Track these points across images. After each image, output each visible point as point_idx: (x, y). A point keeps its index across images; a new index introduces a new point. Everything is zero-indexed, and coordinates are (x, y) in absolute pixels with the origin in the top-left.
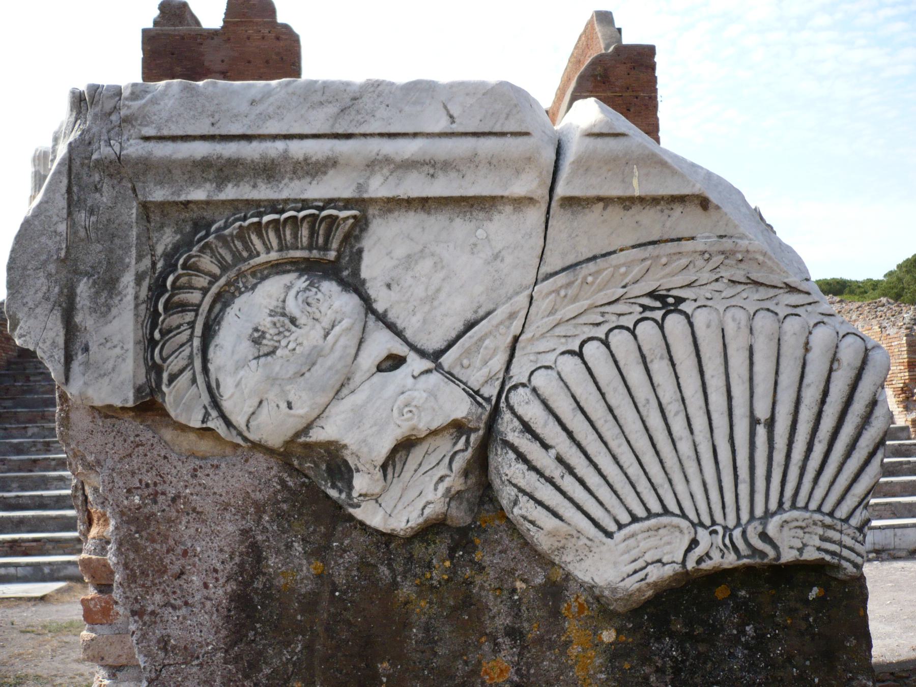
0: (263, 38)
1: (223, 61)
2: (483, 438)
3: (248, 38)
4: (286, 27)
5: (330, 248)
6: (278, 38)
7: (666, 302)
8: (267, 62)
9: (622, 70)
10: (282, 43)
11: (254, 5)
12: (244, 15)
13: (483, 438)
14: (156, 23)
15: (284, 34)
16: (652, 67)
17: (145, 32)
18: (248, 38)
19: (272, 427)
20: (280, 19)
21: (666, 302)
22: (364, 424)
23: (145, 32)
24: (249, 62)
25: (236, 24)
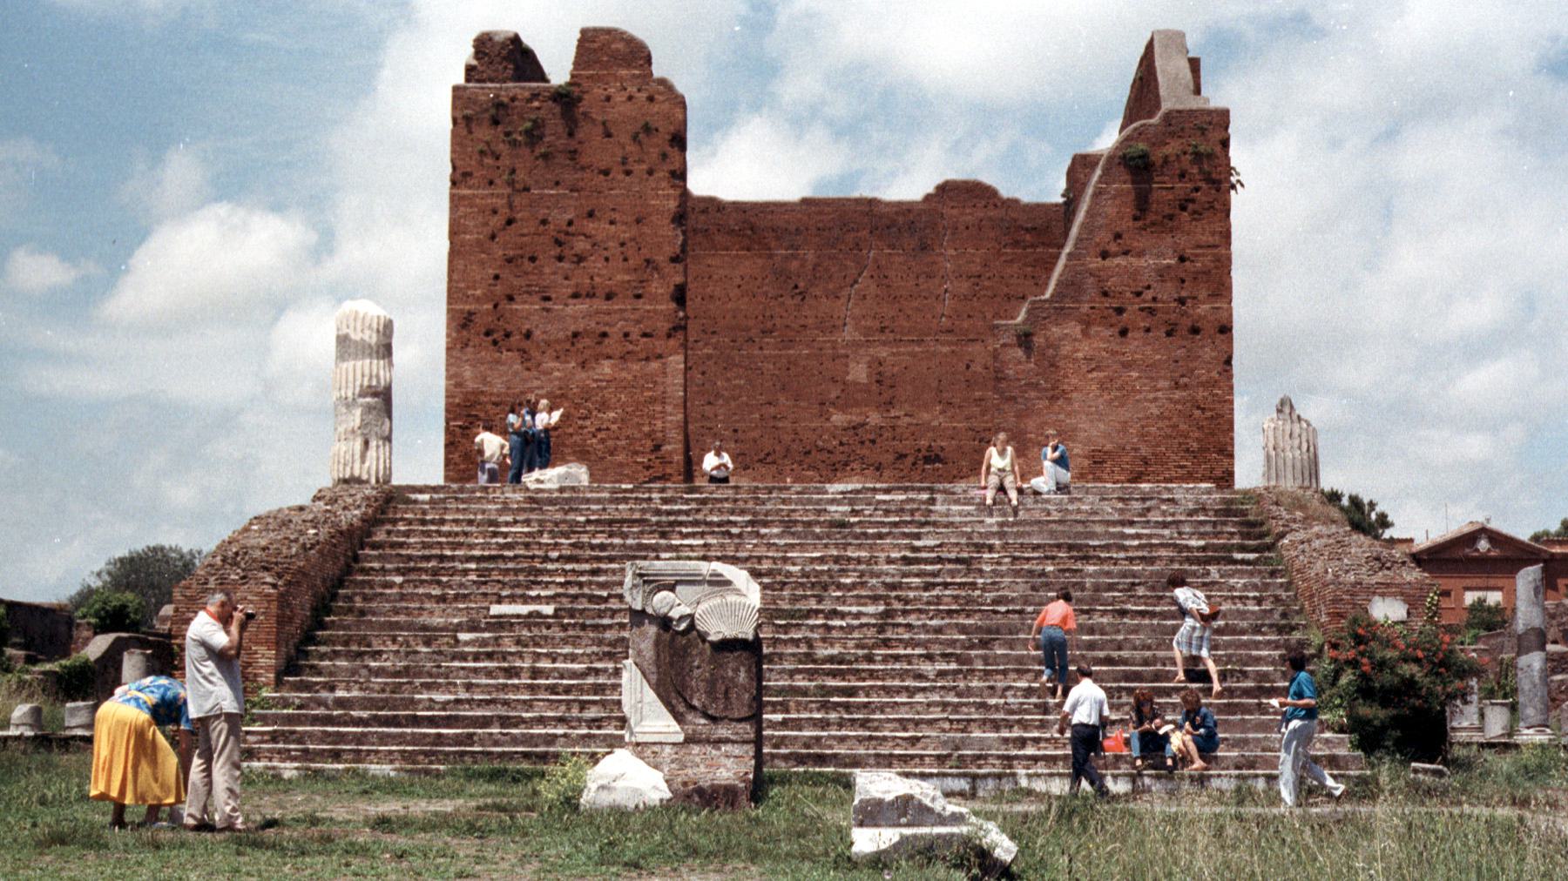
0: (630, 98)
2: (691, 616)
3: (608, 99)
4: (663, 82)
5: (672, 588)
10: (656, 108)
13: (691, 616)
14: (470, 70)
17: (456, 89)
18: (608, 99)
20: (658, 71)
22: (675, 614)
23: (456, 89)
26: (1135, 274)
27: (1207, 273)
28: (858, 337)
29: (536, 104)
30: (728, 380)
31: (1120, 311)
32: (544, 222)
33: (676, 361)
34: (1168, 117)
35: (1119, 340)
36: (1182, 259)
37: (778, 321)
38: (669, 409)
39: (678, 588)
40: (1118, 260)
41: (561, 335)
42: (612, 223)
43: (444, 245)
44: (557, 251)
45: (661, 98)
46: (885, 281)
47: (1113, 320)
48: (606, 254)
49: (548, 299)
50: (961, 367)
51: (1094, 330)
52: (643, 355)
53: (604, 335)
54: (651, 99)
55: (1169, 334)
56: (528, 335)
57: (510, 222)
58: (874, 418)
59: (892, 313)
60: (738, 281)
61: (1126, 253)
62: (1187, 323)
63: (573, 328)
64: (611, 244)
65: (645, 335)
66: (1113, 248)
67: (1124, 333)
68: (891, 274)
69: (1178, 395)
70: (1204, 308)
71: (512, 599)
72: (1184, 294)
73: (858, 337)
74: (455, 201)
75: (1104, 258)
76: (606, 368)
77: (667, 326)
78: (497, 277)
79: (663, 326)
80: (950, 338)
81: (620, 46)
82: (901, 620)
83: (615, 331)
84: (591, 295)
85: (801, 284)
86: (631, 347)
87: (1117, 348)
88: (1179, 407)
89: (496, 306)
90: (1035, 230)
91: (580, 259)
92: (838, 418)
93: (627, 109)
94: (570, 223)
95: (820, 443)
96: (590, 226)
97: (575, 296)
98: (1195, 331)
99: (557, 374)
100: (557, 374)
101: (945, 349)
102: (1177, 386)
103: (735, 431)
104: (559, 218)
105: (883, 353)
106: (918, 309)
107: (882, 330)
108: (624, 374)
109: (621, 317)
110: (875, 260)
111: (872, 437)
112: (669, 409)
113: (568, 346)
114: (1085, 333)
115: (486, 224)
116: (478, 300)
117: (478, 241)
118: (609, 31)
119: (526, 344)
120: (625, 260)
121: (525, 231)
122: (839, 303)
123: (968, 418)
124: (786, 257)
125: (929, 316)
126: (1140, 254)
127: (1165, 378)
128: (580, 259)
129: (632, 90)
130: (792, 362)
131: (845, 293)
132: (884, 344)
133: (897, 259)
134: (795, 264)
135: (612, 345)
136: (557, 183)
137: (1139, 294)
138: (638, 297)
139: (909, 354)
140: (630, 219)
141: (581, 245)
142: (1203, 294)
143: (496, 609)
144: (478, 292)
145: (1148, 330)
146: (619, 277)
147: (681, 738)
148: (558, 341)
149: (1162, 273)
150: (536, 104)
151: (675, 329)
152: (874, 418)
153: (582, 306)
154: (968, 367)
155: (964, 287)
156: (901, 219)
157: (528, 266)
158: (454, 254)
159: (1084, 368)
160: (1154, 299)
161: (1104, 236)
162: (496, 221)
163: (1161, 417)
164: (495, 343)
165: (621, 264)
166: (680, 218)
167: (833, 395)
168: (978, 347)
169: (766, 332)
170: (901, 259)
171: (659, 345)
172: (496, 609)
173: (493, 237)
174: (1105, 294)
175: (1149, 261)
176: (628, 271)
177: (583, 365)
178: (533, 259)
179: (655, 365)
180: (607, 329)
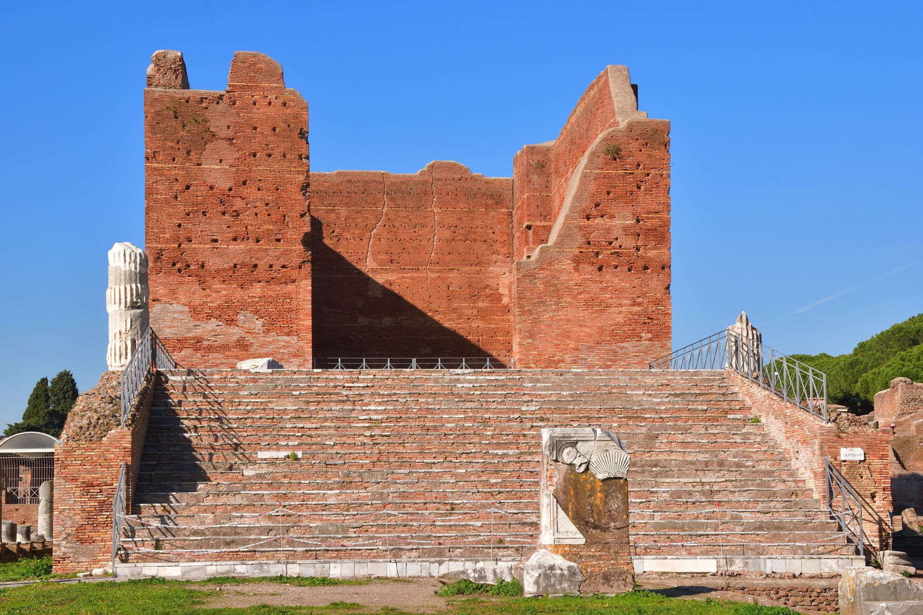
0: (270, 104)
1: (229, 127)
5: (574, 444)
6: (284, 104)
7: (607, 451)
8: (274, 129)
9: (634, 146)
11: (261, 69)
12: (251, 79)
13: (588, 463)
15: (293, 101)
16: (666, 145)
18: (255, 104)
19: (568, 462)
21: (607, 451)
22: (577, 462)
24: (255, 128)
25: (242, 87)
26: (608, 230)
27: (656, 229)
28: (375, 266)
29: (204, 105)
31: (597, 254)
32: (212, 188)
33: (306, 285)
34: (630, 127)
35: (598, 273)
36: (638, 221)
38: (301, 317)
39: (579, 445)
40: (598, 220)
41: (226, 266)
42: (259, 190)
43: (143, 204)
44: (222, 208)
45: (291, 104)
46: (394, 229)
47: (595, 261)
48: (255, 210)
49: (216, 241)
51: (582, 266)
52: (283, 280)
53: (256, 266)
54: (284, 104)
55: (630, 270)
56: (203, 266)
57: (188, 187)
61: (602, 216)
62: (640, 263)
63: (234, 261)
64: (259, 204)
65: (284, 267)
66: (594, 212)
67: (600, 269)
68: (397, 225)
69: (636, 309)
70: (651, 254)
71: (269, 447)
72: (640, 243)
73: (375, 266)
74: (150, 171)
75: (588, 219)
76: (257, 290)
77: (300, 260)
78: (180, 225)
79: (297, 261)
81: (262, 65)
82: (529, 458)
83: (263, 264)
84: (245, 238)
85: (337, 231)
86: (274, 275)
87: (597, 278)
88: (636, 317)
89: (179, 246)
90: (495, 197)
91: (237, 214)
92: (362, 320)
93: (270, 111)
94: (230, 190)
96: (245, 191)
97: (235, 239)
98: (646, 268)
99: (224, 293)
100: (224, 293)
102: (635, 304)
104: (223, 184)
106: (415, 248)
108: (270, 293)
109: (269, 254)
110: (387, 214)
112: (301, 317)
113: (230, 273)
114: (576, 269)
115: (171, 189)
116: (167, 241)
117: (166, 200)
118: (255, 56)
119: (202, 272)
120: (269, 215)
121: (199, 194)
124: (328, 211)
126: (612, 217)
127: (627, 298)
128: (237, 214)
129: (272, 97)
131: (367, 235)
134: (333, 216)
135: (260, 273)
136: (221, 161)
137: (610, 243)
138: (278, 240)
139: (411, 278)
140: (273, 188)
141: (239, 204)
142: (653, 244)
143: (262, 455)
144: (167, 235)
145: (616, 267)
146: (266, 227)
147: (582, 541)
148: (224, 269)
149: (626, 229)
150: (204, 105)
151: (304, 262)
153: (241, 246)
155: (447, 234)
156: (403, 187)
157: (202, 218)
158: (148, 210)
159: (575, 292)
160: (620, 246)
161: (587, 203)
162: (178, 187)
163: (625, 324)
164: (180, 271)
165: (266, 218)
166: (305, 187)
171: (294, 274)
172: (262, 455)
173: (176, 197)
174: (589, 243)
175: (617, 222)
176: (269, 223)
177: (242, 286)
178: (204, 213)
179: (291, 287)
180: (258, 262)
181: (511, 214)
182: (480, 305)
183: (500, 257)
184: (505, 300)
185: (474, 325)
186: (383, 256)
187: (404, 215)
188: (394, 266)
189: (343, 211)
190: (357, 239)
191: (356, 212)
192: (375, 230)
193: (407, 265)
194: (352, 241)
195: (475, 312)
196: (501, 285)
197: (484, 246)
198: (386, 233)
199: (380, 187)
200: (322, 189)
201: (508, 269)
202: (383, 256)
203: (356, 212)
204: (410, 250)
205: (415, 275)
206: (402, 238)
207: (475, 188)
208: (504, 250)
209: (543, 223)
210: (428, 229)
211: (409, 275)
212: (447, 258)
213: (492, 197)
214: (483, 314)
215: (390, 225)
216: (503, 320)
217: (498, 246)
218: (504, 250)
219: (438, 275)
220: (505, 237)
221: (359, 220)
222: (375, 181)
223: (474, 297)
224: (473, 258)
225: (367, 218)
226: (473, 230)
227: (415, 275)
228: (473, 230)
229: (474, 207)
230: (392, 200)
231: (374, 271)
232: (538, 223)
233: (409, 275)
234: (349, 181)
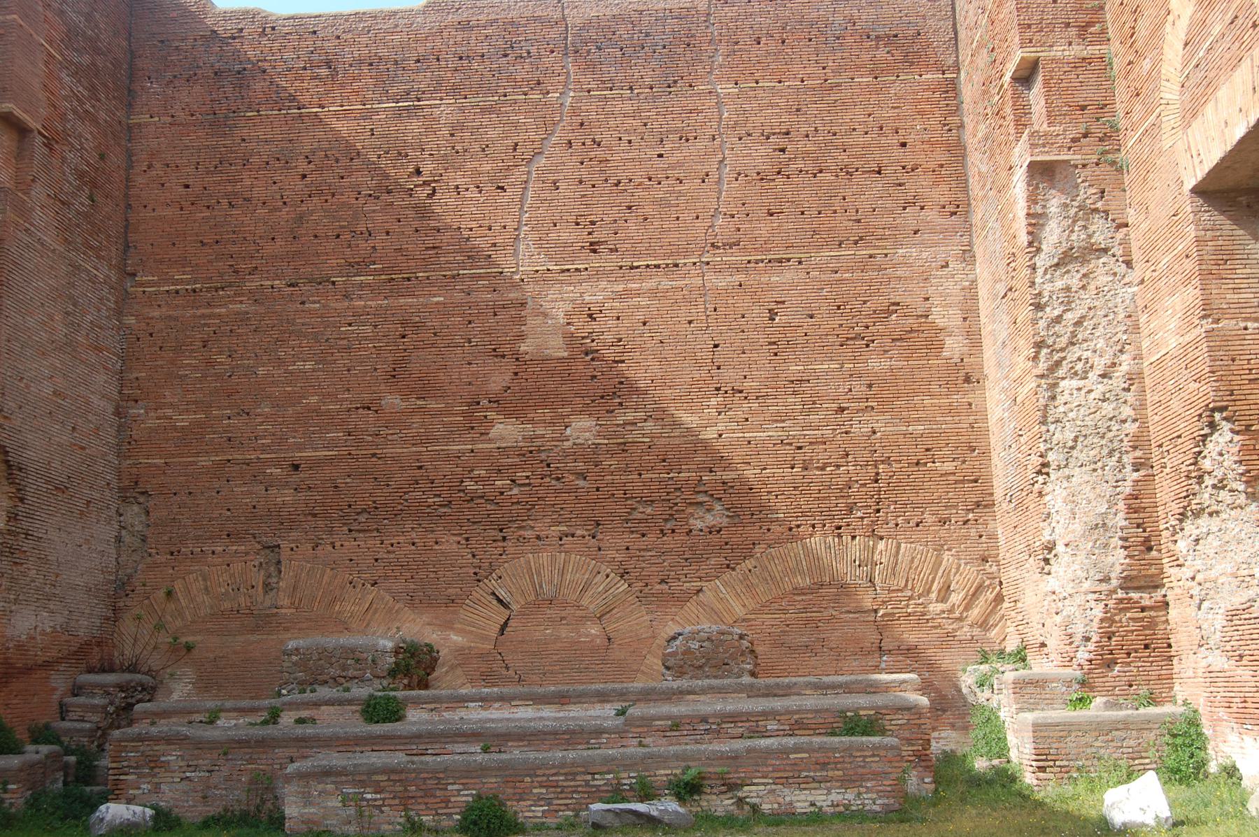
30: (280, 362)
37: (379, 240)
46: (598, 153)
50: (758, 315)
58: (582, 429)
59: (614, 213)
60: (303, 166)
68: (606, 137)
80: (735, 257)
85: (427, 168)
92: (506, 431)
95: (470, 485)
101: (722, 281)
103: (296, 467)
105: (595, 293)
106: (662, 203)
107: (594, 248)
110: (575, 111)
111: (581, 466)
122: (503, 198)
123: (779, 419)
124: (399, 114)
125: (687, 216)
130: (408, 325)
131: (518, 175)
132: (599, 274)
133: (619, 107)
134: (415, 126)
139: (654, 293)
152: (582, 429)
154: (772, 315)
155: (760, 156)
167: (499, 379)
168: (789, 275)
169: (358, 266)
170: (628, 107)
181: (951, 88)
182: (876, 364)
183: (931, 215)
184: (954, 346)
185: (859, 429)
186: (566, 234)
187: (628, 107)
188: (605, 261)
189: (445, 110)
190: (488, 188)
191: (483, 111)
192: (542, 161)
193: (639, 255)
194: (472, 193)
195: (859, 388)
196: (936, 300)
197: (877, 186)
198: (573, 162)
199: (554, 34)
200: (383, 52)
201: (957, 250)
202: (566, 234)
203: (483, 111)
204: (648, 210)
205: (666, 284)
206: (623, 176)
207: (839, 19)
208: (940, 194)
209: (1077, 50)
210: (700, 145)
211: (650, 284)
212: (763, 229)
213: (891, 39)
214: (880, 395)
215: (584, 138)
216: (950, 410)
217: (919, 184)
218: (940, 194)
219: (740, 277)
220: (940, 156)
221: (492, 134)
222: (536, 19)
223: (857, 340)
224: (843, 224)
225: (516, 125)
226: (838, 141)
227: (666, 284)
228: (838, 141)
229: (836, 72)
230: (591, 66)
231: (542, 277)
232: (1057, 52)
233: (650, 284)
234: (465, 26)
